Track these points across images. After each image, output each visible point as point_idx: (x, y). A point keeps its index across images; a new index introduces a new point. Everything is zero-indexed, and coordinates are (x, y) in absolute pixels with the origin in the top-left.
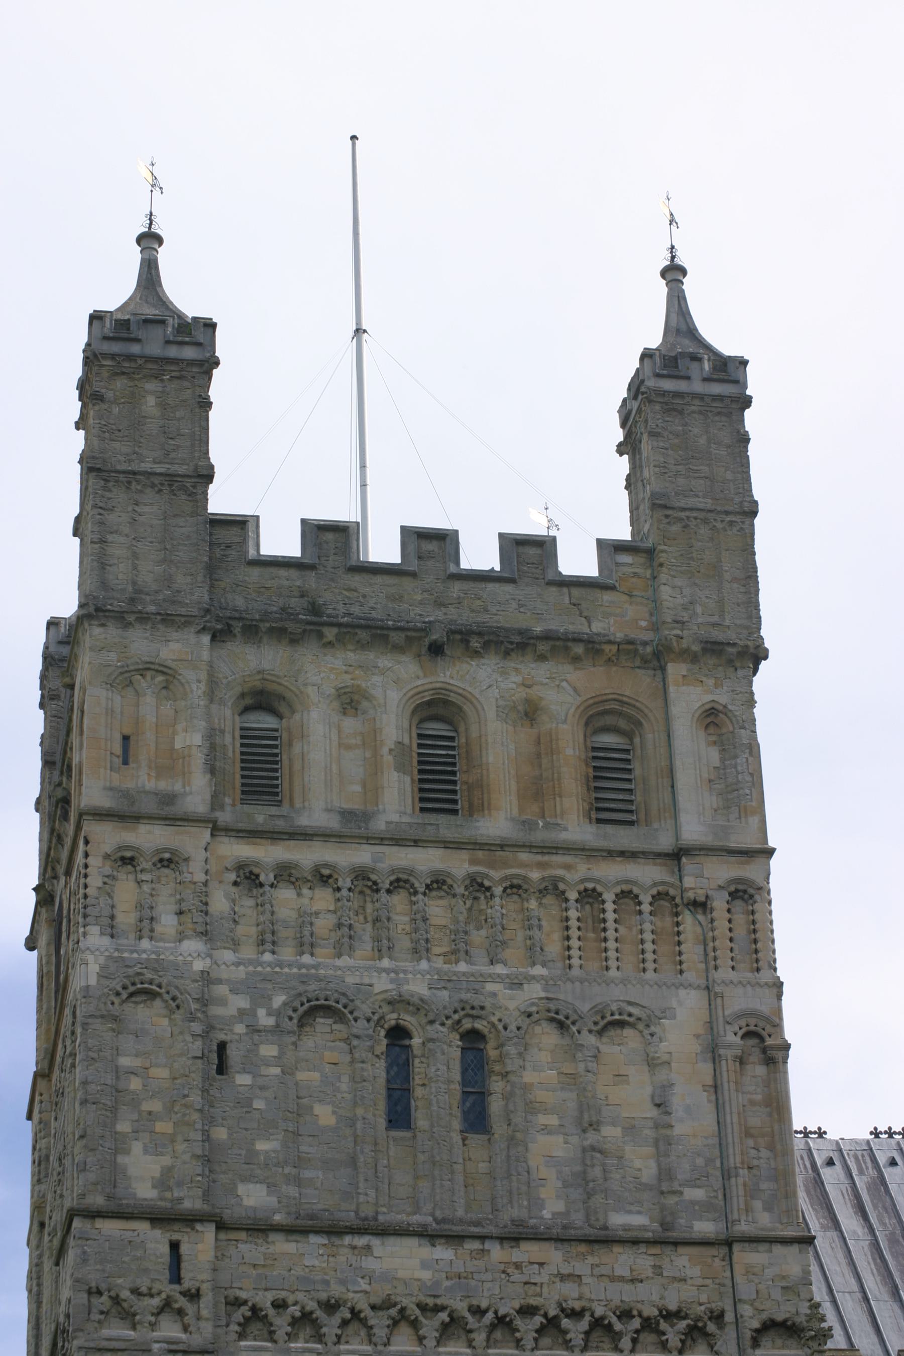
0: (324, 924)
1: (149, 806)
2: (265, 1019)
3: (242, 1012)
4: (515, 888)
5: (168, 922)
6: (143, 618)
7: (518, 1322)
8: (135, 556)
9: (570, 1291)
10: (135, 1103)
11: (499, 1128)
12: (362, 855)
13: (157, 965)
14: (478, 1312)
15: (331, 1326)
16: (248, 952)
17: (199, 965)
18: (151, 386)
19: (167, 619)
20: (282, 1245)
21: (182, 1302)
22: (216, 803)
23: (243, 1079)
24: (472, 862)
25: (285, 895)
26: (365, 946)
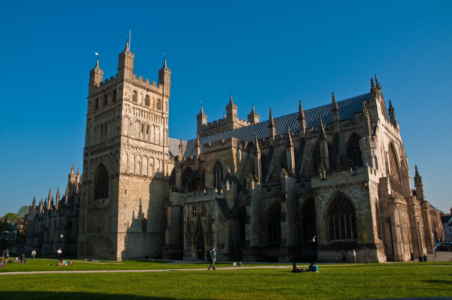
0: (138, 113)
1: (127, 100)
3: (133, 120)
5: (128, 111)
6: (128, 82)
9: (153, 149)
13: (128, 115)
14: (147, 149)
15: (137, 148)
19: (130, 83)
21: (128, 145)
23: (132, 126)
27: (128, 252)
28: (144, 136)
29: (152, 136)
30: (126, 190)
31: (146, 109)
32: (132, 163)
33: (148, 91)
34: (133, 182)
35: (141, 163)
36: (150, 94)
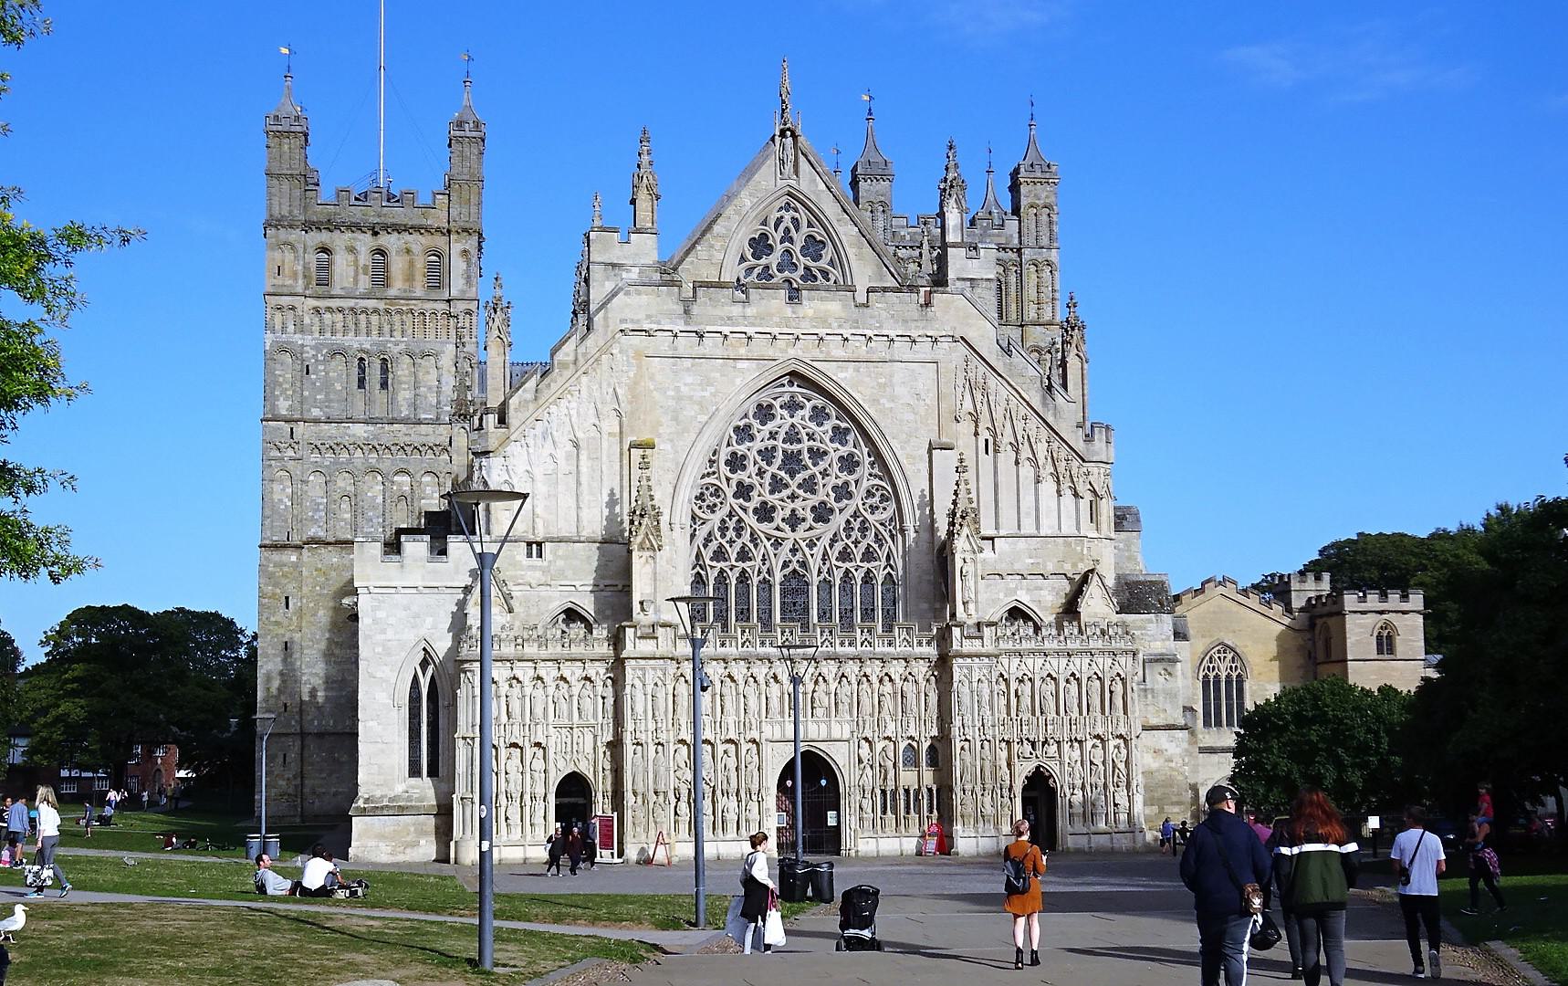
0: (339, 326)
1: (285, 291)
2: (320, 358)
4: (400, 312)
6: (283, 227)
7: (392, 448)
8: (280, 204)
9: (407, 440)
10: (281, 385)
11: (390, 388)
12: (351, 303)
13: (287, 343)
15: (337, 450)
16: (317, 335)
17: (300, 342)
18: (287, 141)
20: (325, 427)
21: (294, 445)
22: (306, 288)
24: (386, 304)
25: (328, 316)
26: (352, 334)
27: (296, 796)
28: (368, 402)
29: (404, 395)
30: (287, 598)
31: (371, 304)
32: (319, 504)
33: (375, 234)
34: (320, 566)
35: (353, 498)
36: (390, 241)
